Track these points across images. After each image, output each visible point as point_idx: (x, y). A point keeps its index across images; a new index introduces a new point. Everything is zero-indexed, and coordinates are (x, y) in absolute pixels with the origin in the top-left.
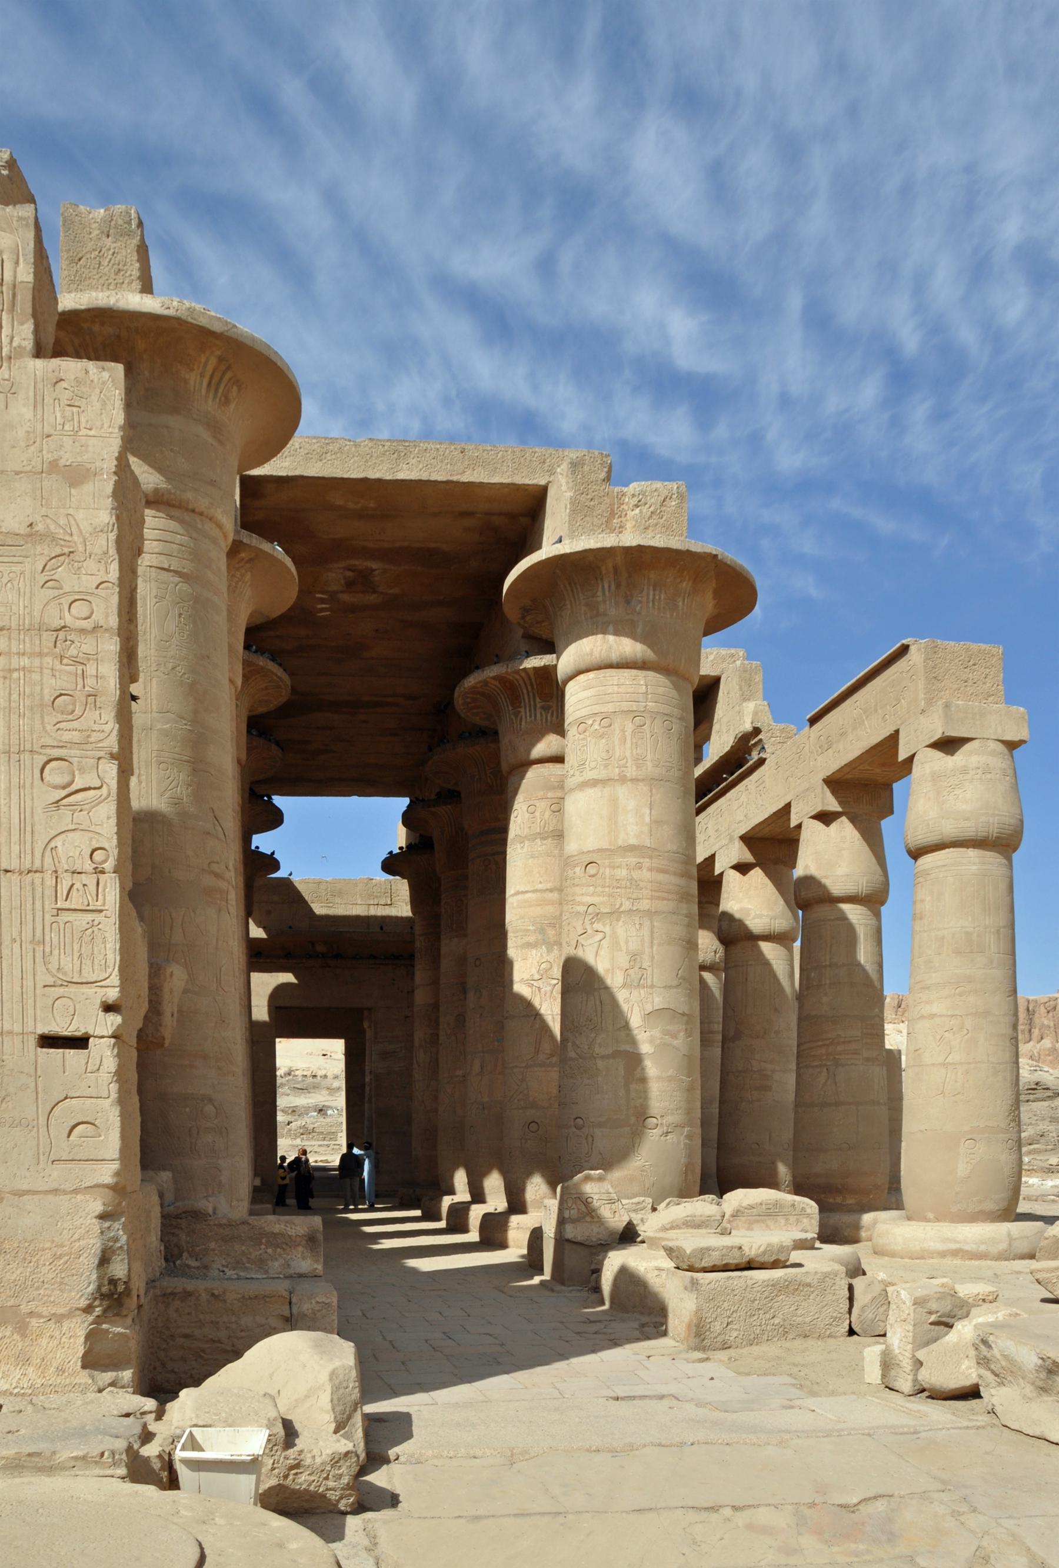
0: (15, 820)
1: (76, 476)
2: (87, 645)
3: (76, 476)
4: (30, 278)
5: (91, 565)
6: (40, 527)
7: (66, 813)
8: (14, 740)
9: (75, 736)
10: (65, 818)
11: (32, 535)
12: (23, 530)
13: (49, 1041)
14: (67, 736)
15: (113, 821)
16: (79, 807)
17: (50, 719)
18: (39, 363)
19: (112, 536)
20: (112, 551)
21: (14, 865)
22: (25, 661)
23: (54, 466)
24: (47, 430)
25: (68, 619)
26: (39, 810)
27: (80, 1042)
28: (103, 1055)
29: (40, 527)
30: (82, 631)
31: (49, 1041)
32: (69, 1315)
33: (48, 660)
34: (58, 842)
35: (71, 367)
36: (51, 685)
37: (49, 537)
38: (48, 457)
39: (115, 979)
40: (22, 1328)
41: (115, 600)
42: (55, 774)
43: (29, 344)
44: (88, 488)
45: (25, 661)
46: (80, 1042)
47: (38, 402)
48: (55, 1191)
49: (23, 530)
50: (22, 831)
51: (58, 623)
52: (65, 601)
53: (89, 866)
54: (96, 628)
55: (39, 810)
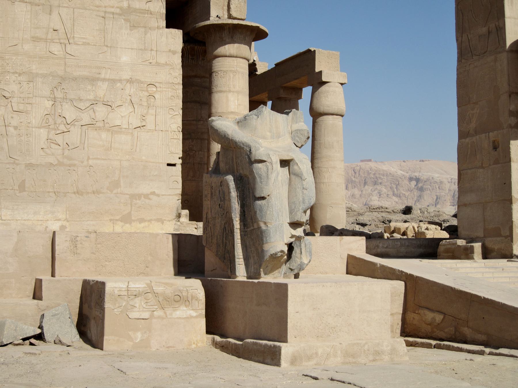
1: (174, 53)
2: (177, 87)
3: (174, 53)
9: (174, 105)
11: (166, 64)
13: (169, 165)
14: (173, 104)
22: (165, 89)
23: (170, 51)
27: (174, 165)
28: (179, 168)
29: (168, 63)
30: (176, 84)
31: (169, 165)
32: (172, 220)
33: (170, 89)
39: (181, 153)
40: (163, 223)
44: (176, 55)
46: (174, 165)
47: (167, 37)
48: (170, 195)
49: (165, 63)
53: (177, 130)
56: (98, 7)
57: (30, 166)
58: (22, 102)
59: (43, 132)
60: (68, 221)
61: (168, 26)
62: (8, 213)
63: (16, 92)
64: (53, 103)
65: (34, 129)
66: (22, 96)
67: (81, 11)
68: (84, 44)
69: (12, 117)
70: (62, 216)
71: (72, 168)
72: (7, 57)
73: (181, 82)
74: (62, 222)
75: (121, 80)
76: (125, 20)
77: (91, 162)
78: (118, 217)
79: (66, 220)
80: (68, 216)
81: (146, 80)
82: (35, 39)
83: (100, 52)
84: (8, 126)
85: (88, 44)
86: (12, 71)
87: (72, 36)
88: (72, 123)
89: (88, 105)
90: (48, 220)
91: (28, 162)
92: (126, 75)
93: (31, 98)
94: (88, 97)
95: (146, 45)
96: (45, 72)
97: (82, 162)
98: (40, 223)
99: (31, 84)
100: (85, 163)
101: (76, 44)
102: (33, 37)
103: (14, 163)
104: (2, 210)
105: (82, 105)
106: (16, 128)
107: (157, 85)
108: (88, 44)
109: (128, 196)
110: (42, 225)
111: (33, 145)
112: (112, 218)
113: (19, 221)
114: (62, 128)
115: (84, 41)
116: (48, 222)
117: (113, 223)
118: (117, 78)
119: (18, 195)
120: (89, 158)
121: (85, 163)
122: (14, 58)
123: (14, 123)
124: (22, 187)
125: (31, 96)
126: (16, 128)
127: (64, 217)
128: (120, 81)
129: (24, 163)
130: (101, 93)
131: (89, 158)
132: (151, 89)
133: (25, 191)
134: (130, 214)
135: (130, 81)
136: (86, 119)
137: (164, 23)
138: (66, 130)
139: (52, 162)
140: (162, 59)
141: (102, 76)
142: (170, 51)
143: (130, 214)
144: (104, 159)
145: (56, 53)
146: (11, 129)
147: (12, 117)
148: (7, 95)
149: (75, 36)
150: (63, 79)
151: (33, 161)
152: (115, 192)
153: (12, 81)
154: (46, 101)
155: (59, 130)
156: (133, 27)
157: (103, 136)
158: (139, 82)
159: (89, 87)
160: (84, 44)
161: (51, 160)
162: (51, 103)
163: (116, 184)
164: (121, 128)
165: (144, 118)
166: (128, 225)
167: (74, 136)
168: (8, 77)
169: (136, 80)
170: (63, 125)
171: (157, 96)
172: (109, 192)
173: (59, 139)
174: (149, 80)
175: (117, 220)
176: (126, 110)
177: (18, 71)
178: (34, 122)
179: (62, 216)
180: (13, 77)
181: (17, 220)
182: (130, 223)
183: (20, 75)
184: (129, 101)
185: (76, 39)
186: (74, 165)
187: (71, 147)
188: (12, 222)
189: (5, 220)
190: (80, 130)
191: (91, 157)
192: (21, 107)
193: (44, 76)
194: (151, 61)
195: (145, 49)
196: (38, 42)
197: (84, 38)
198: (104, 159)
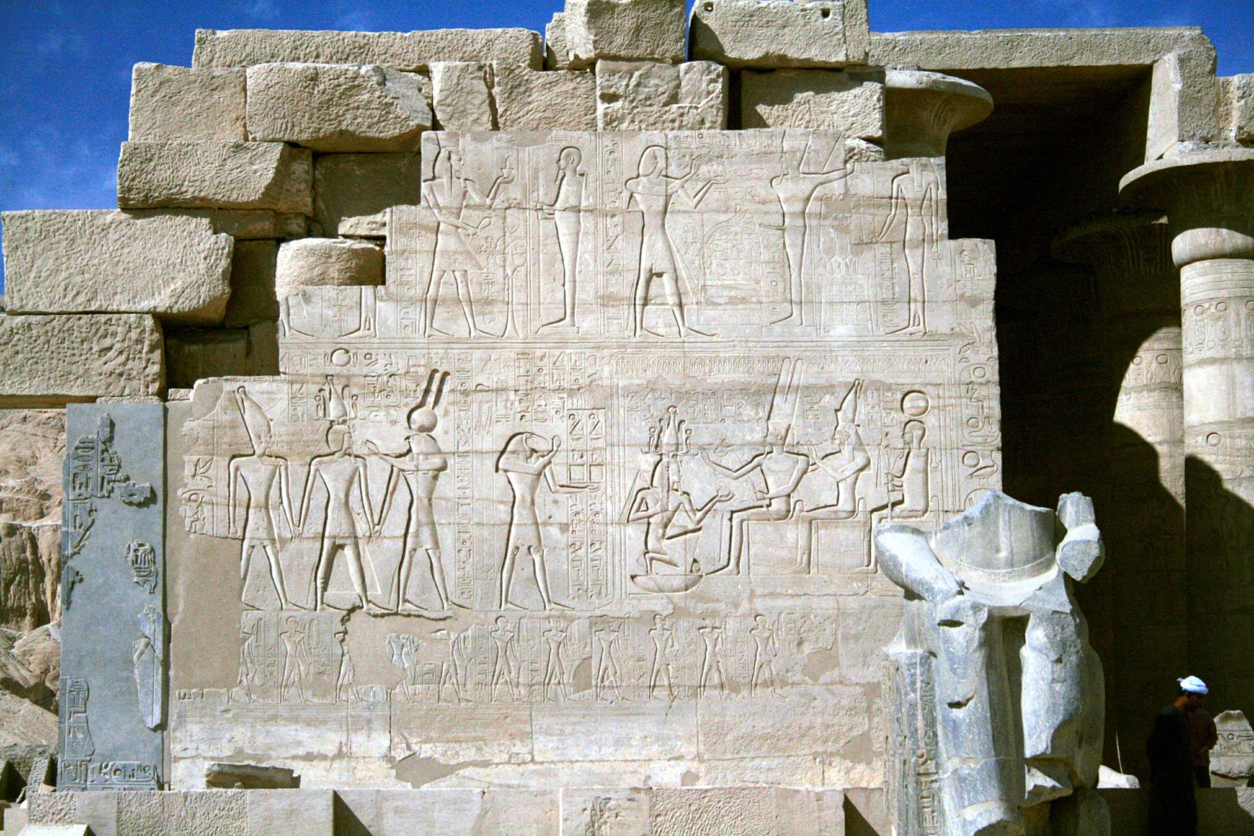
0: (950, 484)
1: (974, 302)
2: (983, 391)
3: (974, 302)
4: (945, 197)
5: (983, 349)
6: (957, 330)
7: (975, 480)
8: (948, 443)
10: (976, 483)
11: (953, 334)
12: (948, 332)
14: (975, 440)
15: (1000, 483)
16: (984, 477)
17: (966, 431)
18: (952, 242)
19: (994, 333)
20: (994, 341)
21: (950, 508)
22: (953, 401)
24: (958, 278)
25: (973, 379)
26: (962, 479)
29: (957, 330)
30: (981, 384)
34: (972, 495)
35: (967, 243)
36: (967, 412)
37: (961, 335)
38: (959, 292)
41: (997, 367)
42: (969, 460)
43: (946, 232)
44: (980, 307)
45: (953, 401)
50: (954, 489)
51: (968, 380)
52: (971, 369)
54: (988, 382)
55: (962, 479)
56: (764, 203)
57: (600, 622)
58: (580, 461)
59: (634, 533)
60: (701, 761)
61: (954, 234)
62: (550, 745)
63: (564, 438)
64: (658, 458)
65: (610, 529)
66: (579, 445)
67: (723, 217)
68: (732, 301)
69: (556, 502)
70: (689, 749)
71: (707, 622)
72: (539, 353)
73: (996, 378)
74: (689, 764)
75: (832, 386)
76: (835, 228)
77: (759, 604)
78: (831, 747)
79: (699, 757)
80: (702, 747)
81: (900, 381)
82: (606, 300)
83: (775, 318)
84: (545, 524)
85: (743, 300)
86: (552, 387)
87: (701, 283)
88: (707, 508)
89: (747, 457)
90: (650, 760)
91: (598, 613)
92: (844, 373)
93: (600, 449)
94: (748, 438)
95: (897, 289)
96: (637, 382)
97: (736, 606)
98: (631, 767)
99: (601, 415)
100: (745, 607)
101: (711, 303)
102: (602, 297)
103: (562, 616)
104: (535, 736)
105: (732, 459)
106: (564, 527)
107: (930, 390)
108: (743, 300)
109: (859, 689)
110: (635, 772)
111: (610, 568)
112: (820, 749)
113: (578, 765)
114: (682, 520)
115: (733, 293)
116: (652, 765)
117: (823, 762)
118: (822, 381)
119: (573, 697)
120: (752, 595)
121: (745, 607)
122: (557, 352)
123: (561, 516)
124: (582, 676)
125: (601, 443)
126: (564, 527)
127: (693, 749)
128: (830, 388)
129: (588, 614)
130: (778, 422)
131: (752, 595)
132: (915, 404)
133: (589, 686)
134: (865, 738)
135: (855, 387)
136: (743, 492)
137: (943, 227)
138: (691, 526)
139: (658, 608)
140: (941, 321)
141: (784, 379)
142: (962, 296)
143: (865, 738)
144: (792, 596)
145: (661, 331)
146: (554, 531)
147: (556, 502)
148: (542, 446)
149: (709, 283)
150: (684, 395)
151: (612, 610)
152: (823, 679)
153: (553, 412)
154: (640, 456)
155: (674, 526)
156: (861, 245)
157: (789, 535)
158: (880, 387)
159: (748, 412)
160: (732, 301)
161: (658, 604)
162: (653, 458)
163: (828, 658)
164: (836, 512)
165: (897, 482)
166: (861, 767)
167: (713, 539)
168: (543, 403)
169: (873, 382)
170: (684, 514)
171: (930, 420)
172: (809, 681)
173: (674, 548)
174: (907, 380)
175: (832, 754)
176: (846, 463)
177: (566, 385)
178: (609, 511)
179: (689, 749)
180: (555, 401)
181: (572, 762)
182: (869, 763)
183: (572, 392)
184: (853, 439)
185: (711, 291)
186: (714, 614)
187: (704, 567)
188: (560, 766)
189: (542, 763)
190: (726, 523)
191: (759, 591)
192: (578, 474)
193: (630, 393)
194: (911, 329)
195: (894, 301)
196: (613, 306)
197: (731, 288)
198: (792, 596)
